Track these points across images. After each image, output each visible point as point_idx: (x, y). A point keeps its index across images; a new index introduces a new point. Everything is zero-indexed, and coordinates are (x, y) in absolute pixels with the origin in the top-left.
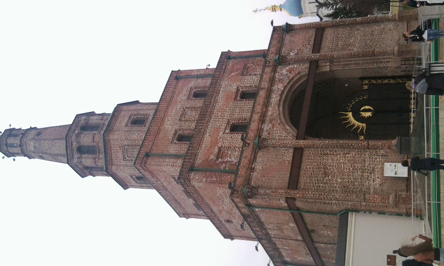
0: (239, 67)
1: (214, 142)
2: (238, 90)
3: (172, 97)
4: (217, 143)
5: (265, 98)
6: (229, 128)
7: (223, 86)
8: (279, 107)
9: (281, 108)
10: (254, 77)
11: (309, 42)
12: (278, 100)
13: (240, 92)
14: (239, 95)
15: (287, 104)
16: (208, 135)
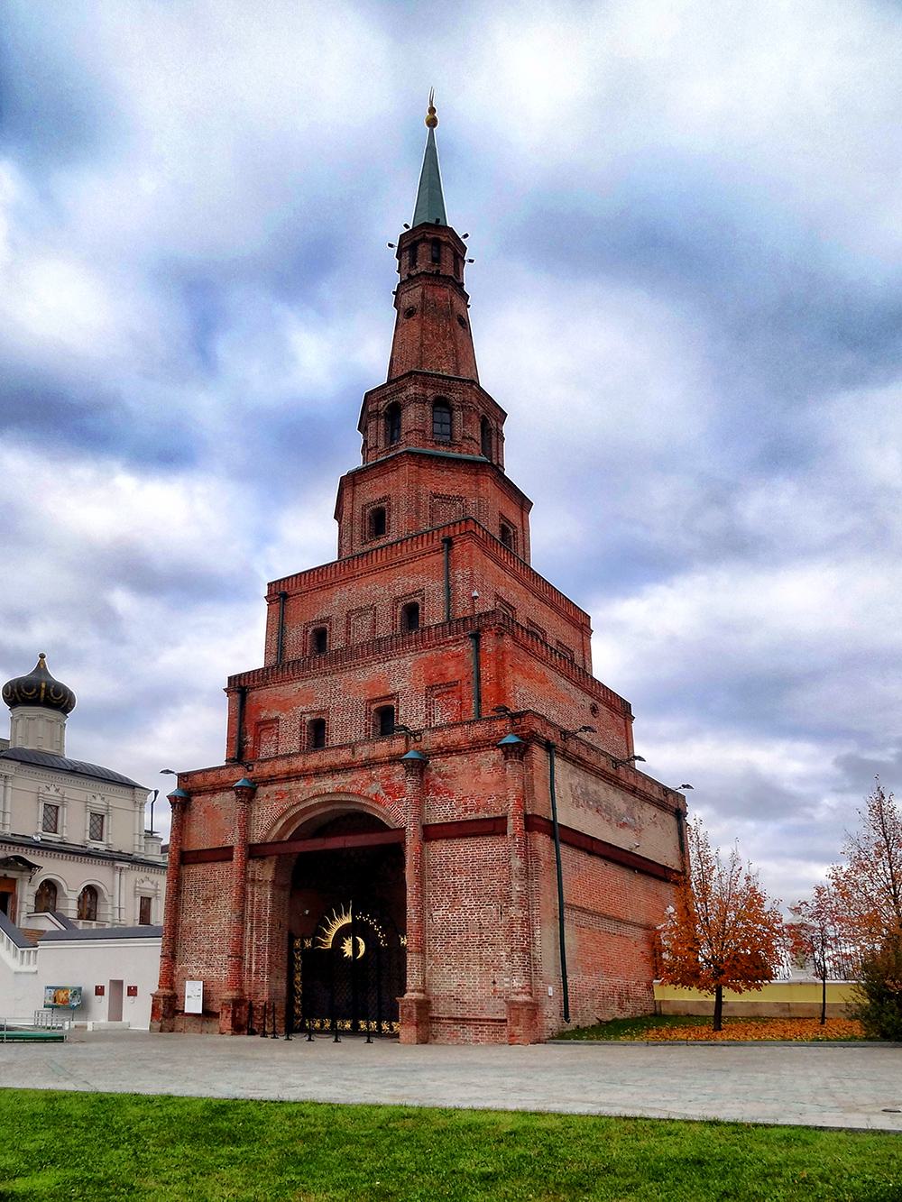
0: (452, 671)
1: (285, 705)
2: (391, 697)
3: (401, 564)
4: (285, 710)
5: (330, 766)
6: (314, 716)
7: (403, 661)
8: (313, 797)
9: (317, 800)
10: (421, 717)
11: (471, 811)
12: (328, 790)
13: (389, 703)
14: (383, 703)
15: (337, 807)
16: (301, 687)
